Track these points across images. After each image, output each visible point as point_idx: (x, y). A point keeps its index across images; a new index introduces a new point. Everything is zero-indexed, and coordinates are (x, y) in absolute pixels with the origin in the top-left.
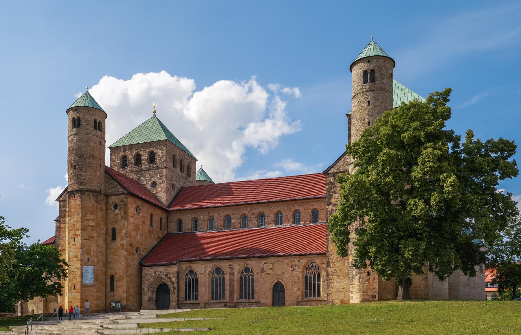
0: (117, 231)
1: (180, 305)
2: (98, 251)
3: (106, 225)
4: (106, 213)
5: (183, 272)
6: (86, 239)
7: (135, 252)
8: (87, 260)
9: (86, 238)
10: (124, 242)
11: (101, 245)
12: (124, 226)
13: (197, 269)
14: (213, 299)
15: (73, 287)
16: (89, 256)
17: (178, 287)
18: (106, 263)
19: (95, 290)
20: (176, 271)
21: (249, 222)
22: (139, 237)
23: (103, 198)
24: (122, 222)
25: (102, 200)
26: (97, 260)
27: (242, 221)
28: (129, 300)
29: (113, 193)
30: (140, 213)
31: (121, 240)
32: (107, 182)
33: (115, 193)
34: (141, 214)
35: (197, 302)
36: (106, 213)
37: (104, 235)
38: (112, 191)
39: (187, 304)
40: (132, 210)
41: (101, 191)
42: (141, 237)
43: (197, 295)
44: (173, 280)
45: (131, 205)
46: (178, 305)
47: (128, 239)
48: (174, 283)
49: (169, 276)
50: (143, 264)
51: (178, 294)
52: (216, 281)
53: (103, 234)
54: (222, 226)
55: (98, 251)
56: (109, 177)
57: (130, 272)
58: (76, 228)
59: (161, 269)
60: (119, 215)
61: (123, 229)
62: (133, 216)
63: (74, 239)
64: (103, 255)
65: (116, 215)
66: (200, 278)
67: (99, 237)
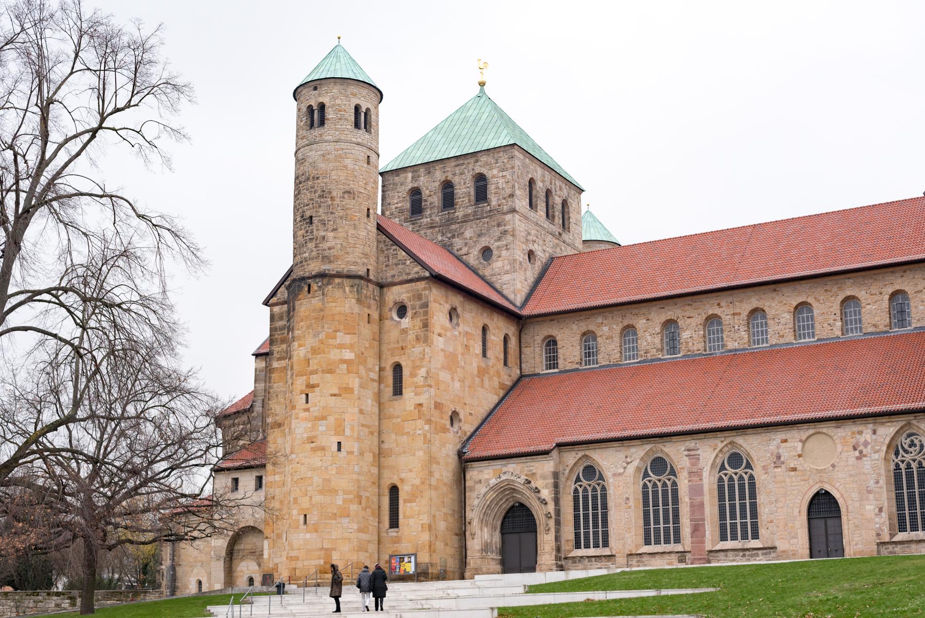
0: (406, 372)
1: (563, 563)
3: (380, 358)
4: (380, 329)
7: (448, 425)
10: (423, 399)
12: (422, 359)
13: (605, 463)
15: (302, 518)
16: (340, 439)
17: (558, 512)
18: (380, 455)
19: (355, 527)
20: (552, 470)
21: (728, 336)
22: (457, 385)
23: (374, 291)
24: (418, 350)
27: (709, 334)
28: (435, 551)
30: (458, 324)
31: (416, 394)
32: (383, 251)
34: (463, 328)
36: (380, 329)
37: (376, 384)
38: (392, 272)
40: (439, 318)
42: (461, 386)
43: (606, 535)
44: (546, 494)
46: (559, 563)
47: (432, 390)
48: (546, 504)
50: (469, 454)
51: (558, 531)
52: (655, 493)
53: (373, 380)
54: (658, 350)
57: (437, 475)
58: (310, 368)
60: (411, 332)
61: (419, 367)
62: (442, 332)
63: (307, 395)
64: (372, 433)
65: (404, 331)
66: (612, 488)
67: (363, 388)
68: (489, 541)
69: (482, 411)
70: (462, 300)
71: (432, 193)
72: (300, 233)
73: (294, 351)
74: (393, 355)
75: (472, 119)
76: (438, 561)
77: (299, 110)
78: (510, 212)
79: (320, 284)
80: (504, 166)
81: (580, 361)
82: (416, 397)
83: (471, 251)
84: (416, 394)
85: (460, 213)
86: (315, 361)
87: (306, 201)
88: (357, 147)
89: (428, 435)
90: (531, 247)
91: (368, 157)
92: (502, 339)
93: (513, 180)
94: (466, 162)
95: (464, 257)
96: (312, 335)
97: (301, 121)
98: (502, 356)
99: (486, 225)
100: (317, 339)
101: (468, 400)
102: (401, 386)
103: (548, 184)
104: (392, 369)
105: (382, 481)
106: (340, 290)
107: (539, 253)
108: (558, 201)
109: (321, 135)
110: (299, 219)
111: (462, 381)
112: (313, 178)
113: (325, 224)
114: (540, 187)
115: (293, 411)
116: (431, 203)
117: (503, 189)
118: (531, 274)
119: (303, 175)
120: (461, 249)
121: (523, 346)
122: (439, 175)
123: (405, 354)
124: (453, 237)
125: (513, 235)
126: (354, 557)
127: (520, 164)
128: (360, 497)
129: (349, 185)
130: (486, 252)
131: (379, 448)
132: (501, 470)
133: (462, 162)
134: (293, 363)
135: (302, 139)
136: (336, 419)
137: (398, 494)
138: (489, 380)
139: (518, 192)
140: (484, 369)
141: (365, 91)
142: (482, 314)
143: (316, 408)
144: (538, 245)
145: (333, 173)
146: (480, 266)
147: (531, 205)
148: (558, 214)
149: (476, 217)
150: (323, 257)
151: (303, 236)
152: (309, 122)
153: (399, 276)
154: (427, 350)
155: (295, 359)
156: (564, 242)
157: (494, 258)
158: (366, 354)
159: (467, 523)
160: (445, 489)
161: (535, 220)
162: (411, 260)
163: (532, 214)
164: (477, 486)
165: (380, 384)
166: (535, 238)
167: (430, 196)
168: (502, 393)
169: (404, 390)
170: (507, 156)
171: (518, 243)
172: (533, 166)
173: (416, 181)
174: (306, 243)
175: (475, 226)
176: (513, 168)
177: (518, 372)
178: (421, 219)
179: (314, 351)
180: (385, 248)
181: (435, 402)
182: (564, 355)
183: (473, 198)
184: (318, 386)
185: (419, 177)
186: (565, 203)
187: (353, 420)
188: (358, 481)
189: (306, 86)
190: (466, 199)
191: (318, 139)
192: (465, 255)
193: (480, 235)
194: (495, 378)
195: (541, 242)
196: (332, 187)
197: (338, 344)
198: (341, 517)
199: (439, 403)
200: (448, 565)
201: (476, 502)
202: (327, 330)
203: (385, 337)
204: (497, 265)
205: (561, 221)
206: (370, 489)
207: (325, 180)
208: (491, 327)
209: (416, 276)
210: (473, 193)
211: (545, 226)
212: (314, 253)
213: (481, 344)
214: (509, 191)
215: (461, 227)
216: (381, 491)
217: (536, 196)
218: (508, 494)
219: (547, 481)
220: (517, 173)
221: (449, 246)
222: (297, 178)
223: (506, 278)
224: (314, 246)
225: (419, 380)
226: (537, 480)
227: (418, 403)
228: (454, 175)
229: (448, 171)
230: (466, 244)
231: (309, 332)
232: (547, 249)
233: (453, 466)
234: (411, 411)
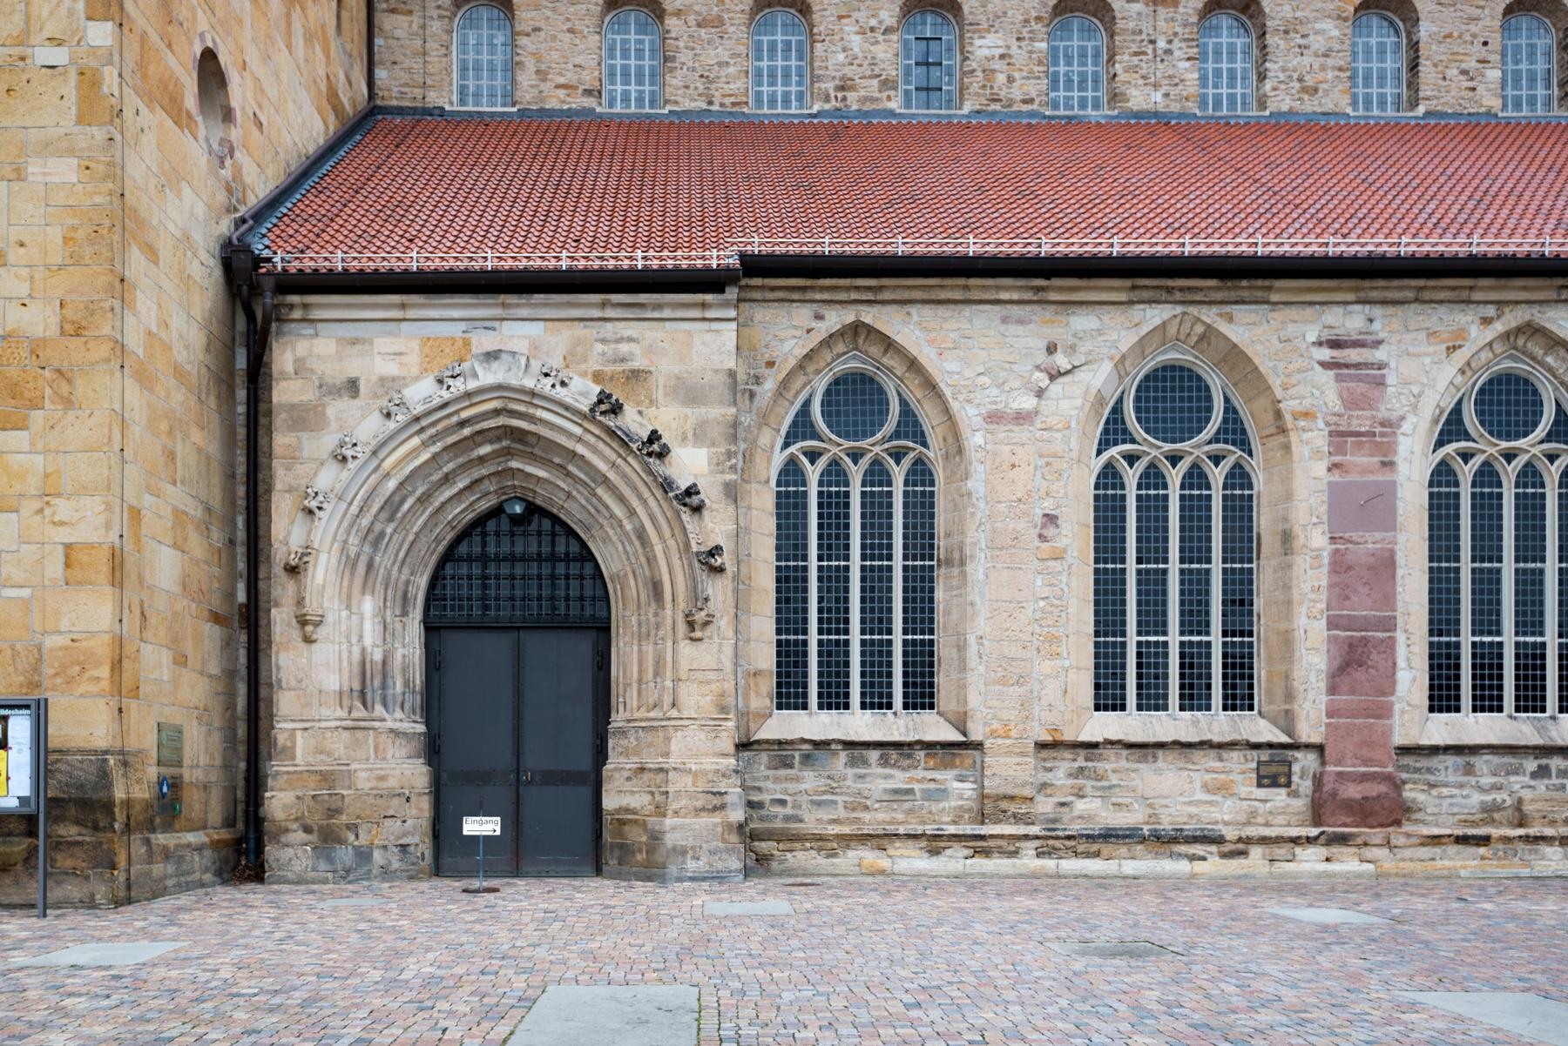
5: (769, 385)
14: (1108, 698)
35: (930, 725)
39: (820, 745)
59: (536, 329)
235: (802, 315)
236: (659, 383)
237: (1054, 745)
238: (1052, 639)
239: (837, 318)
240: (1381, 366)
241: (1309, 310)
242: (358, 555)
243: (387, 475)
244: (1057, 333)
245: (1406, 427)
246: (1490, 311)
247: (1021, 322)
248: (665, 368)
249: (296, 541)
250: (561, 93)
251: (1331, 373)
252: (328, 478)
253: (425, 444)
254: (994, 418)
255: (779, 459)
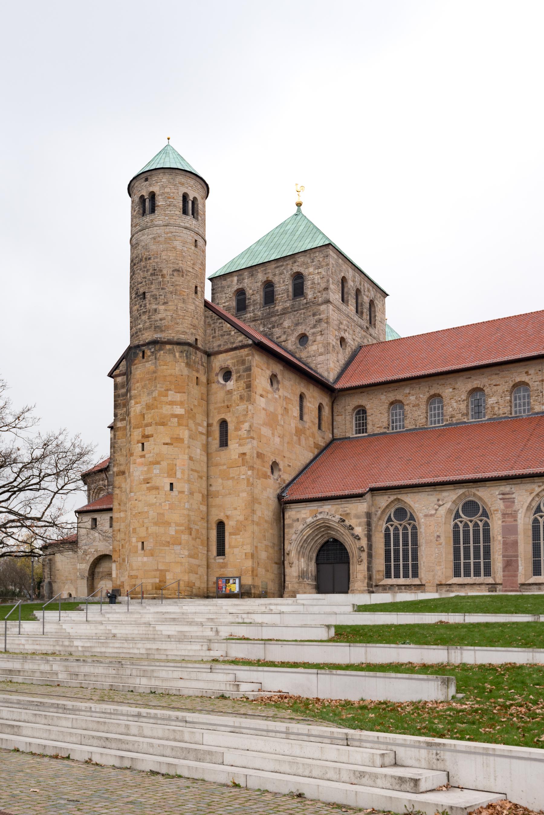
0: (231, 427)
2: (192, 470)
3: (208, 416)
4: (208, 391)
5: (379, 512)
6: (167, 444)
8: (168, 487)
9: (167, 442)
10: (246, 449)
11: (198, 457)
12: (246, 415)
19: (186, 553)
22: (277, 440)
23: (201, 358)
24: (242, 407)
25: (200, 362)
26: (190, 488)
29: (222, 348)
30: (278, 389)
31: (240, 445)
32: (210, 325)
33: (226, 347)
34: (281, 392)
35: (416, 581)
36: (208, 391)
37: (204, 437)
38: (219, 343)
41: (196, 343)
43: (416, 568)
45: (260, 370)
47: (255, 442)
49: (347, 523)
51: (370, 563)
53: (201, 433)
55: (192, 470)
56: (214, 315)
57: (259, 513)
60: (235, 393)
61: (243, 422)
62: (264, 393)
63: (143, 444)
64: (201, 477)
65: (229, 392)
68: (305, 569)
69: (299, 464)
70: (282, 368)
71: (255, 292)
72: (135, 308)
73: (131, 407)
74: (219, 413)
75: (290, 231)
76: (260, 584)
77: (133, 202)
78: (324, 303)
79: (153, 350)
80: (320, 264)
81: (387, 426)
82: (240, 448)
83: (289, 338)
84: (240, 445)
85: (279, 307)
86: (150, 416)
87: (139, 280)
88: (185, 231)
89: (251, 479)
90: (343, 334)
91: (196, 241)
92: (317, 407)
93: (328, 275)
94: (285, 264)
95: (283, 343)
96: (146, 394)
97: (135, 211)
98: (317, 421)
99: (302, 316)
100: (151, 397)
101: (287, 454)
102: (227, 439)
103: (358, 284)
104: (218, 425)
105: (211, 518)
106: (171, 355)
107: (349, 340)
108: (366, 300)
109: (152, 221)
110: (133, 296)
111: (281, 437)
112: (146, 259)
113: (156, 298)
114: (351, 286)
115: (132, 458)
116: (254, 301)
117: (318, 284)
118: (342, 357)
119: (137, 257)
120: (280, 337)
121: (335, 414)
122: (261, 277)
123: (230, 412)
124: (273, 327)
125: (327, 323)
126: (186, 578)
127: (334, 263)
128: (190, 529)
129: (178, 264)
130: (303, 339)
131: (207, 491)
132: (317, 510)
133: (281, 264)
134: (130, 418)
135: (135, 226)
136: (168, 464)
137: (224, 528)
138: (305, 439)
139: (332, 287)
140: (301, 430)
141: (192, 182)
142: (299, 384)
143: (151, 455)
144: (349, 334)
145: (163, 254)
146: (297, 350)
147: (343, 300)
148: (366, 311)
149: (294, 309)
150: (155, 327)
151: (138, 310)
152: (141, 211)
153: (224, 345)
154: (250, 407)
155: (132, 414)
156: (371, 335)
157: (310, 342)
158: (195, 411)
159: (286, 554)
160: (266, 526)
161: (347, 313)
162: (236, 331)
163: (343, 307)
164: (295, 524)
165: (208, 437)
166: (346, 328)
167: (253, 295)
168: (316, 452)
169: (229, 442)
170: (323, 255)
171: (331, 329)
172: (345, 267)
173: (241, 283)
174: (140, 315)
175: (293, 317)
176: (328, 265)
177: (331, 436)
178: (245, 314)
179: (149, 407)
180: (211, 322)
181: (258, 453)
182: (372, 421)
183: (291, 294)
184: (152, 436)
185: (243, 279)
186: (372, 303)
187: (184, 465)
188: (188, 515)
189: (138, 178)
190: (285, 295)
191: (149, 224)
192: (284, 341)
193: (297, 324)
194: (310, 438)
195: (351, 332)
196: (163, 265)
197: (170, 401)
198: (173, 544)
199: (261, 454)
200: (269, 587)
201: (294, 537)
202: (160, 389)
203: (213, 399)
204: (312, 348)
205: (368, 317)
206: (199, 523)
207: (156, 260)
208: (307, 396)
209: (240, 344)
210: (291, 289)
211: (355, 319)
212: (147, 324)
213: (298, 408)
214: (323, 285)
215: (280, 319)
216: (209, 526)
217: (347, 293)
218: (323, 531)
219: (360, 520)
220: (332, 270)
221: (270, 335)
222: (132, 261)
223: (320, 359)
224: (147, 318)
225: (243, 433)
226: (351, 519)
227: (242, 452)
228: (275, 275)
229: (269, 273)
230: (285, 333)
231: (144, 392)
232: (356, 339)
233: (273, 507)
234: (236, 459)
235: (386, 497)
236: (352, 515)
237: (441, 585)
238: (439, 562)
239: (392, 498)
240: (514, 498)
241: (497, 487)
242: (300, 551)
243: (304, 536)
244: (440, 497)
245: (520, 511)
246: (541, 484)
247: (432, 495)
248: (353, 512)
249: (288, 550)
250: (378, 429)
251: (502, 501)
252: (294, 537)
253: (311, 529)
254: (426, 516)
255: (384, 526)
